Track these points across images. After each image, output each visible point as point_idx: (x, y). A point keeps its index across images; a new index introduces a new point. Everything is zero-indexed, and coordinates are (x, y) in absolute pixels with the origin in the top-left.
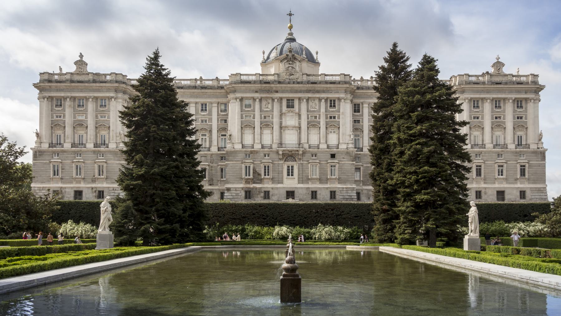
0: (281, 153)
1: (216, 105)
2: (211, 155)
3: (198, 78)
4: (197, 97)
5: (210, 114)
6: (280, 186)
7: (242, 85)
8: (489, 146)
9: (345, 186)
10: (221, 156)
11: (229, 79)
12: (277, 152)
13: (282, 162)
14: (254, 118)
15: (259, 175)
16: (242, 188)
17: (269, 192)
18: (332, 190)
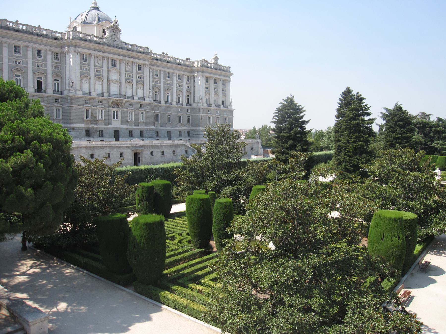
0: (112, 101)
1: (50, 53)
2: (48, 97)
3: (37, 26)
4: (34, 43)
5: (45, 60)
6: (109, 126)
7: (82, 42)
8: (214, 105)
9: (148, 128)
10: (56, 98)
11: (65, 32)
12: (108, 101)
13: (111, 108)
14: (89, 71)
15: (95, 117)
16: (84, 128)
17: (102, 131)
18: (141, 130)
